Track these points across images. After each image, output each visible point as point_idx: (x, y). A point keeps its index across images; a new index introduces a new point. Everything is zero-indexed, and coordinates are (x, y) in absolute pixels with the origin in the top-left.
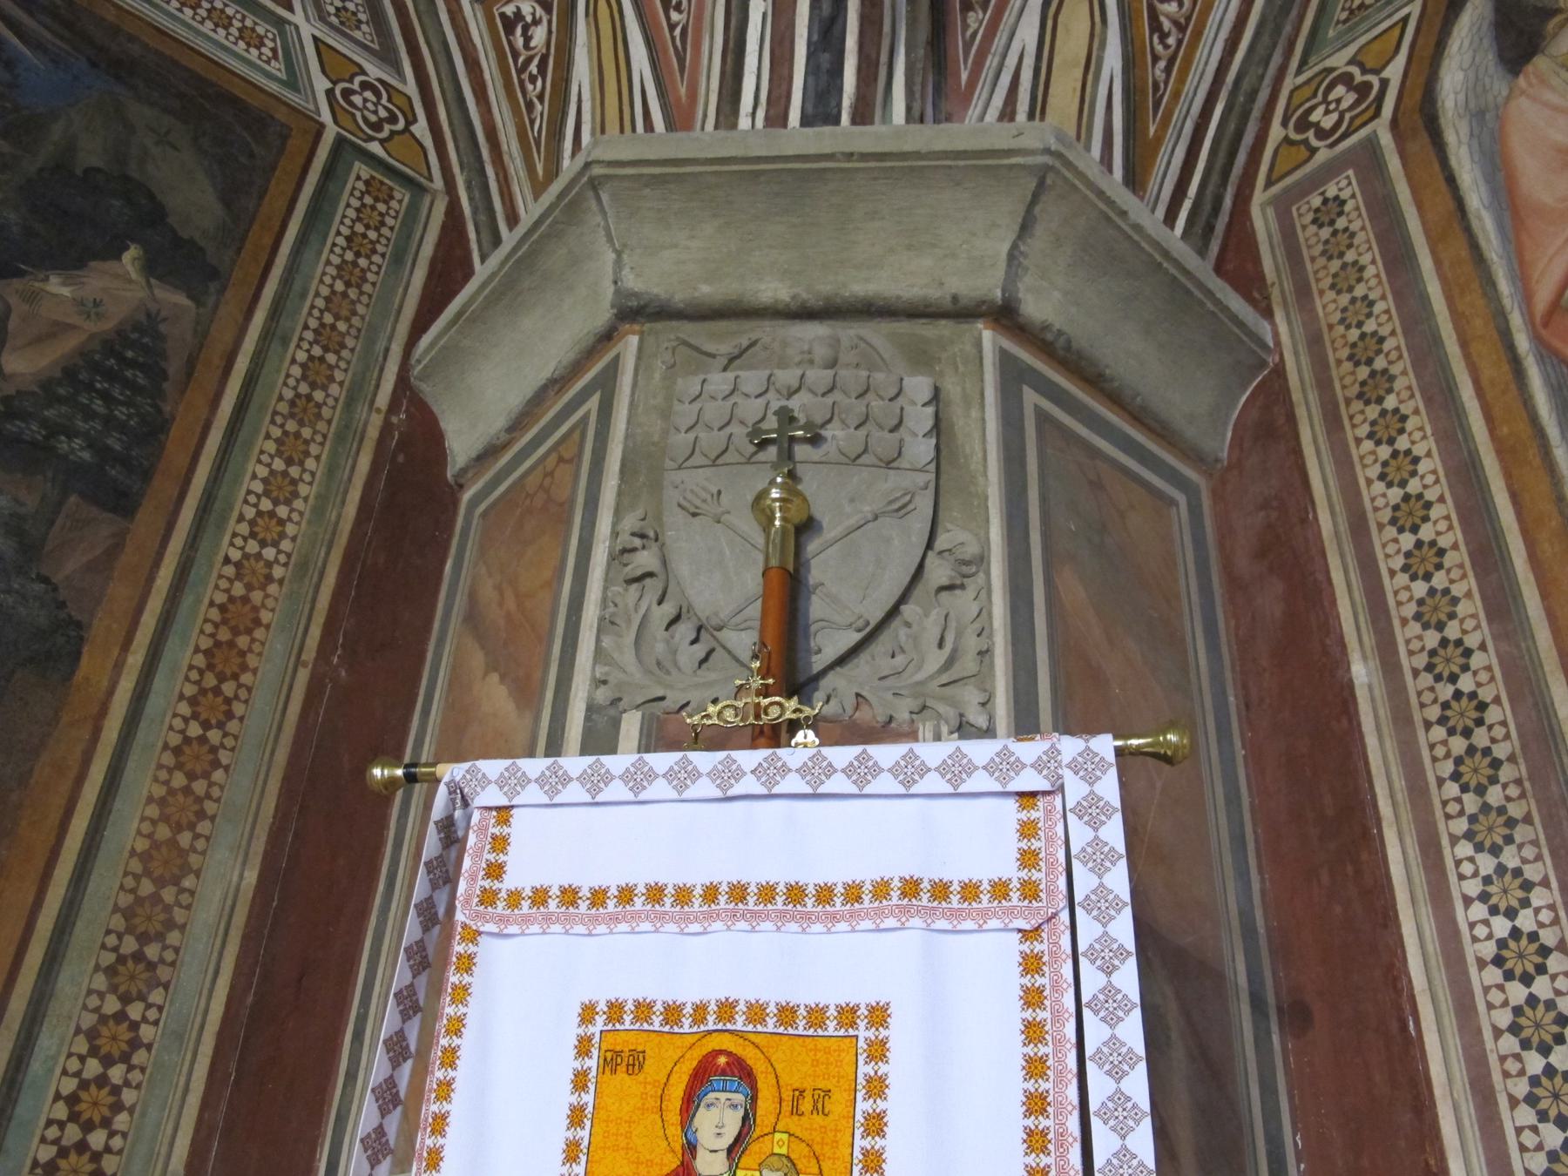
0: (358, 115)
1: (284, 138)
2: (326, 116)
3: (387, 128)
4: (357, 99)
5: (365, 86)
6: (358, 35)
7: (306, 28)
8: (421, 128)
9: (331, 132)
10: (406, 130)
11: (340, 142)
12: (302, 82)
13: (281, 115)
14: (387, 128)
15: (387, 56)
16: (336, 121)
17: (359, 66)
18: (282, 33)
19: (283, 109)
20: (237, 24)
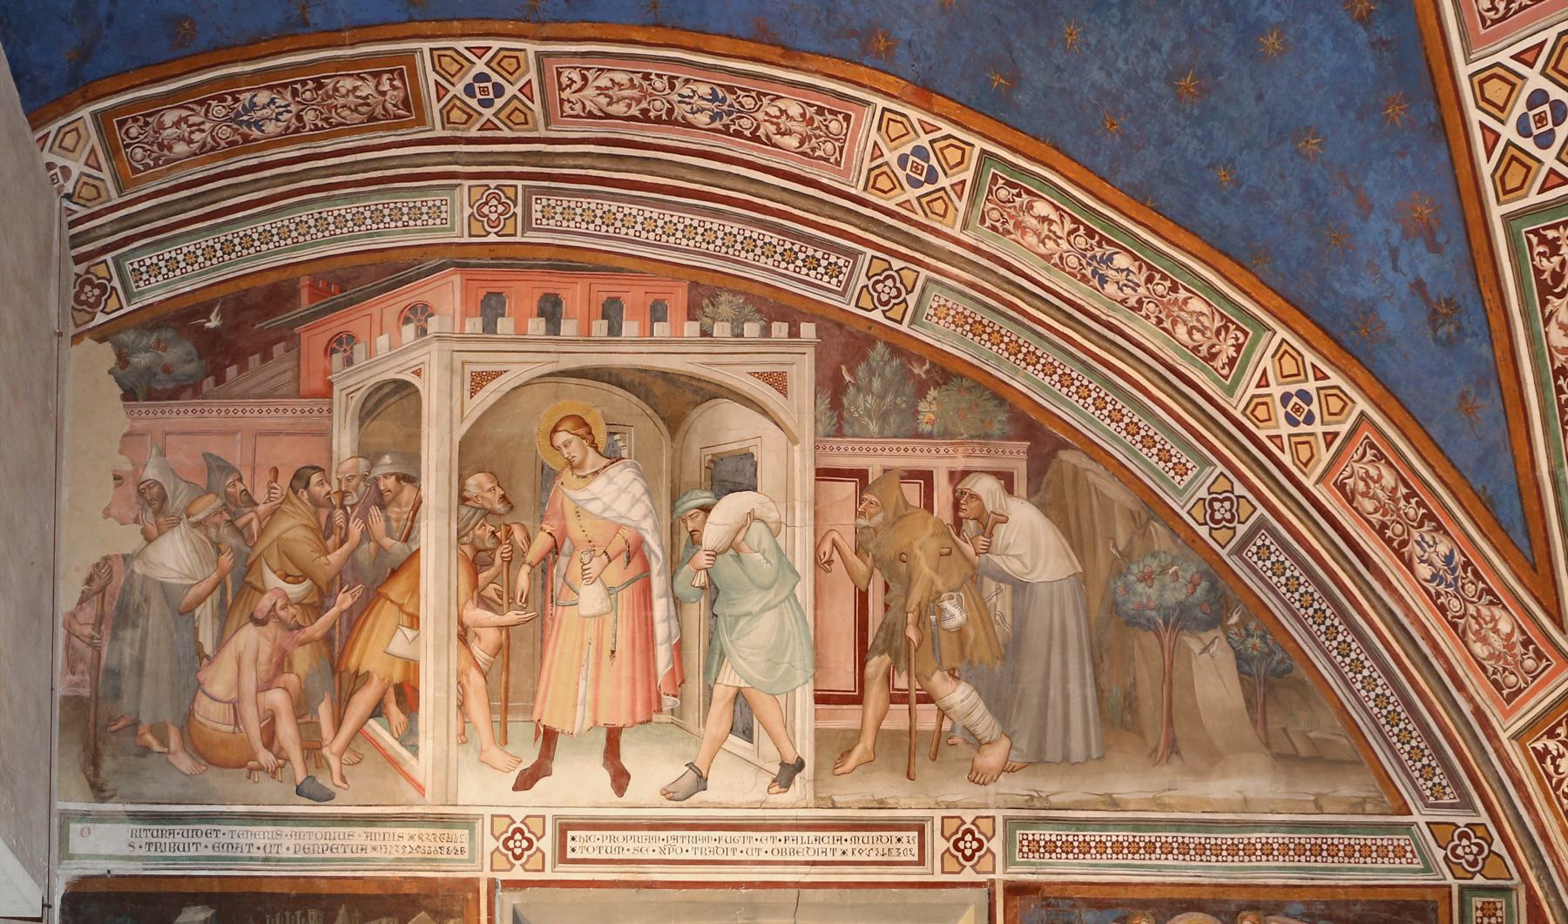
0: (1463, 861)
1: (1435, 910)
2: (1450, 880)
3: (1480, 858)
4: (1460, 851)
5: (1463, 835)
6: (1446, 800)
7: (1420, 817)
8: (1498, 846)
9: (1455, 884)
10: (1490, 851)
11: (1462, 888)
12: (1432, 863)
13: (1430, 896)
14: (1480, 858)
15: (1466, 804)
16: (1455, 878)
17: (1453, 824)
18: (1412, 835)
19: (1429, 890)
20: (1390, 848)
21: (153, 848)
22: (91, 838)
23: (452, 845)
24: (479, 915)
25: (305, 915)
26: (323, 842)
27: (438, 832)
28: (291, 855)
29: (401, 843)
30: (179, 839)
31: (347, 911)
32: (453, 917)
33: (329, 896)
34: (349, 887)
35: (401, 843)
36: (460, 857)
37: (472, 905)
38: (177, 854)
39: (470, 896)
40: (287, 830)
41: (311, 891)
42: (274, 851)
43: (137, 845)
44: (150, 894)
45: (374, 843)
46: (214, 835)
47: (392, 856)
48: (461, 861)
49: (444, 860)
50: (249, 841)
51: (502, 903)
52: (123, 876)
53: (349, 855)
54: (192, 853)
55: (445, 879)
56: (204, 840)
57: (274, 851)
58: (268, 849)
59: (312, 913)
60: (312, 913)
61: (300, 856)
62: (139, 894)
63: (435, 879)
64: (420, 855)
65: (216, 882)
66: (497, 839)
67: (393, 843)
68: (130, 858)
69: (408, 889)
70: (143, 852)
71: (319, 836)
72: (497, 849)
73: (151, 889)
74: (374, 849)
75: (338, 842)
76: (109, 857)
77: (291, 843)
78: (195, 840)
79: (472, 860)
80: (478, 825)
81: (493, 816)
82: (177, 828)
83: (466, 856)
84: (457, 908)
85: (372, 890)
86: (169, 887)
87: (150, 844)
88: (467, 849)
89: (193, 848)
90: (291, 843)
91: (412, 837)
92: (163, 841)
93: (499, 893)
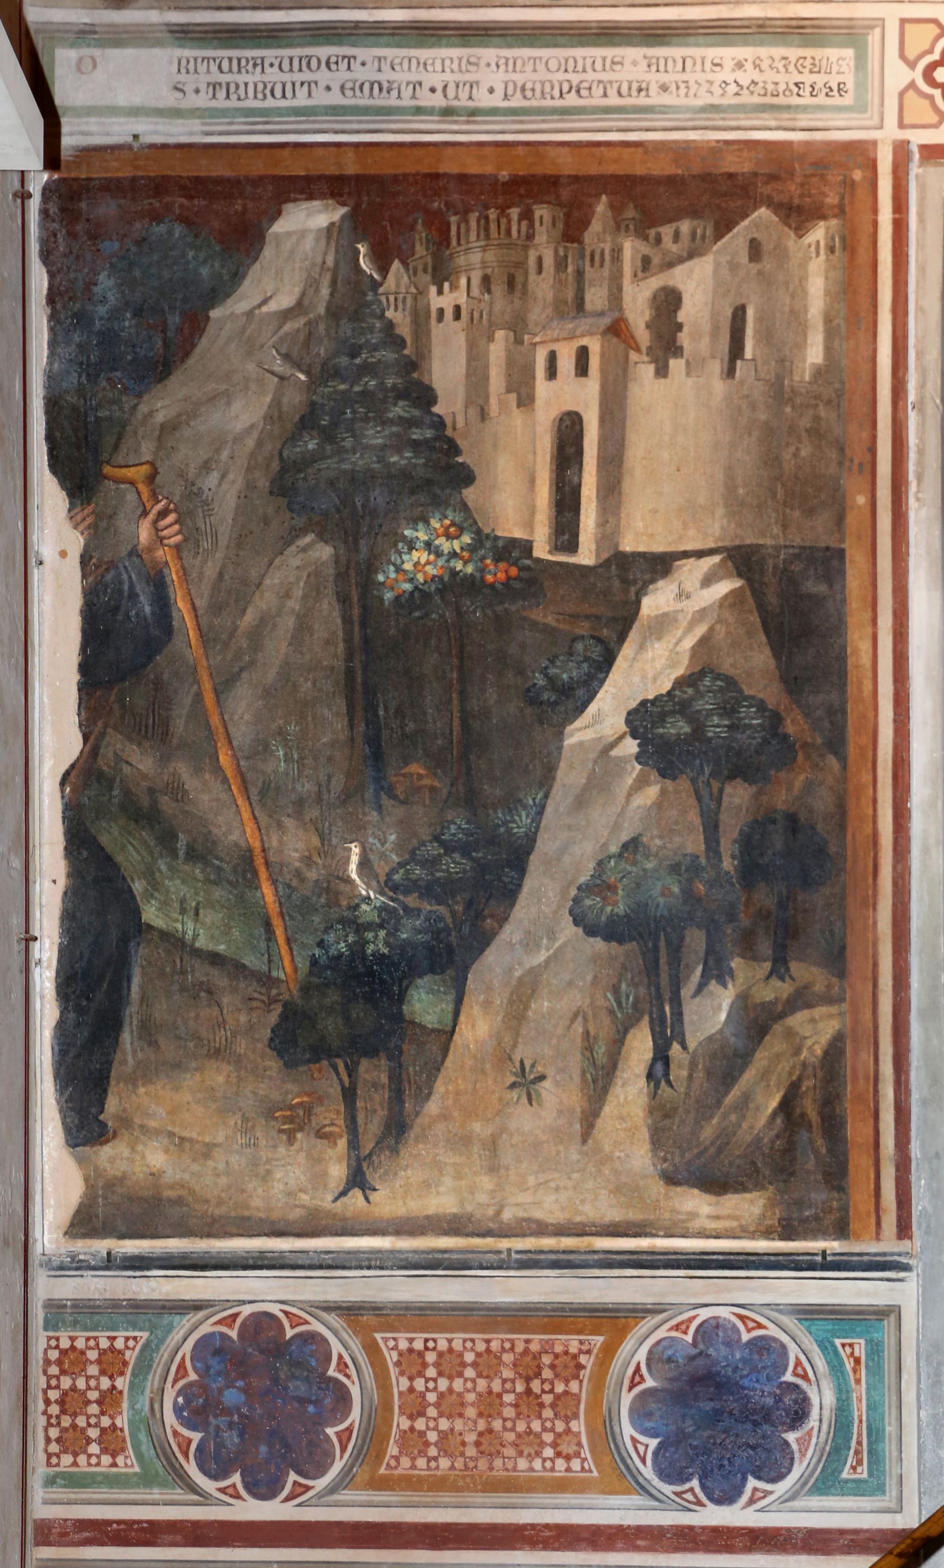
21: (222, 94)
22: (99, 75)
23: (820, 79)
24: (875, 210)
25: (527, 215)
26: (561, 76)
27: (793, 53)
28: (497, 101)
29: (719, 76)
30: (272, 75)
31: (612, 207)
32: (824, 217)
33: (576, 179)
34: (615, 161)
35: (719, 76)
36: (837, 101)
37: (862, 193)
38: (270, 103)
39: (857, 175)
40: (489, 54)
41: (539, 170)
42: (464, 94)
43: (189, 89)
44: (219, 181)
45: (663, 78)
46: (343, 65)
47: (700, 102)
48: (839, 109)
49: (805, 109)
50: (414, 77)
51: (922, 188)
52: (165, 146)
53: (613, 100)
54: (301, 100)
55: (807, 143)
56: (323, 76)
57: (464, 94)
58: (451, 92)
59: (542, 212)
60: (542, 212)
61: (517, 102)
62: (197, 180)
63: (788, 144)
64: (756, 100)
65: (350, 154)
66: (912, 65)
67: (702, 77)
68: (176, 113)
69: (731, 164)
70: (203, 101)
71: (553, 65)
72: (912, 85)
73: (221, 170)
74: (664, 88)
75: (590, 76)
76: (135, 112)
77: (497, 79)
78: (307, 76)
79: (860, 107)
80: (874, 38)
81: (903, 21)
82: (270, 54)
83: (848, 100)
84: (832, 199)
85: (661, 167)
86: (257, 167)
87: (215, 86)
88: (850, 86)
89: (302, 92)
90: (497, 79)
91: (740, 65)
92: (241, 78)
93: (915, 169)
